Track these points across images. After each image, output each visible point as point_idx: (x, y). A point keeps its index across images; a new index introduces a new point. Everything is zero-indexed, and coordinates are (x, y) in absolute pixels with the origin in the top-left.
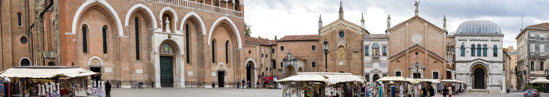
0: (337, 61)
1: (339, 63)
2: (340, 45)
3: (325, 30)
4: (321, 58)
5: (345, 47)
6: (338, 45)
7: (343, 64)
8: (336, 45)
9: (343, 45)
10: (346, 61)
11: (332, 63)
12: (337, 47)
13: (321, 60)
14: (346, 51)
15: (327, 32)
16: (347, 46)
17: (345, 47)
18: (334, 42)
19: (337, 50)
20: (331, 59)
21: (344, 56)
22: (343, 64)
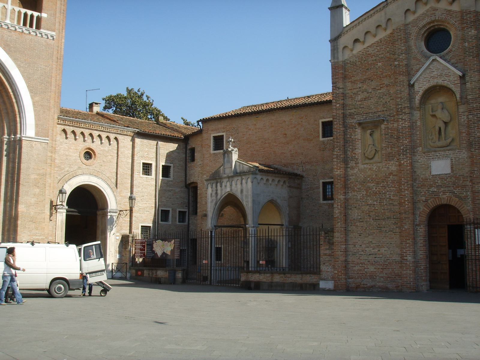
0: (420, 159)
1: (429, 167)
2: (433, 82)
3: (358, 33)
4: (345, 152)
5: (457, 90)
6: (420, 88)
7: (448, 171)
8: (411, 86)
9: (445, 83)
10: (464, 155)
11: (394, 168)
12: (418, 98)
13: (346, 162)
14: (462, 109)
15: (370, 41)
16: (468, 85)
17: (457, 90)
18: (401, 78)
19: (419, 108)
20: (389, 150)
21: (452, 132)
22: (448, 171)
